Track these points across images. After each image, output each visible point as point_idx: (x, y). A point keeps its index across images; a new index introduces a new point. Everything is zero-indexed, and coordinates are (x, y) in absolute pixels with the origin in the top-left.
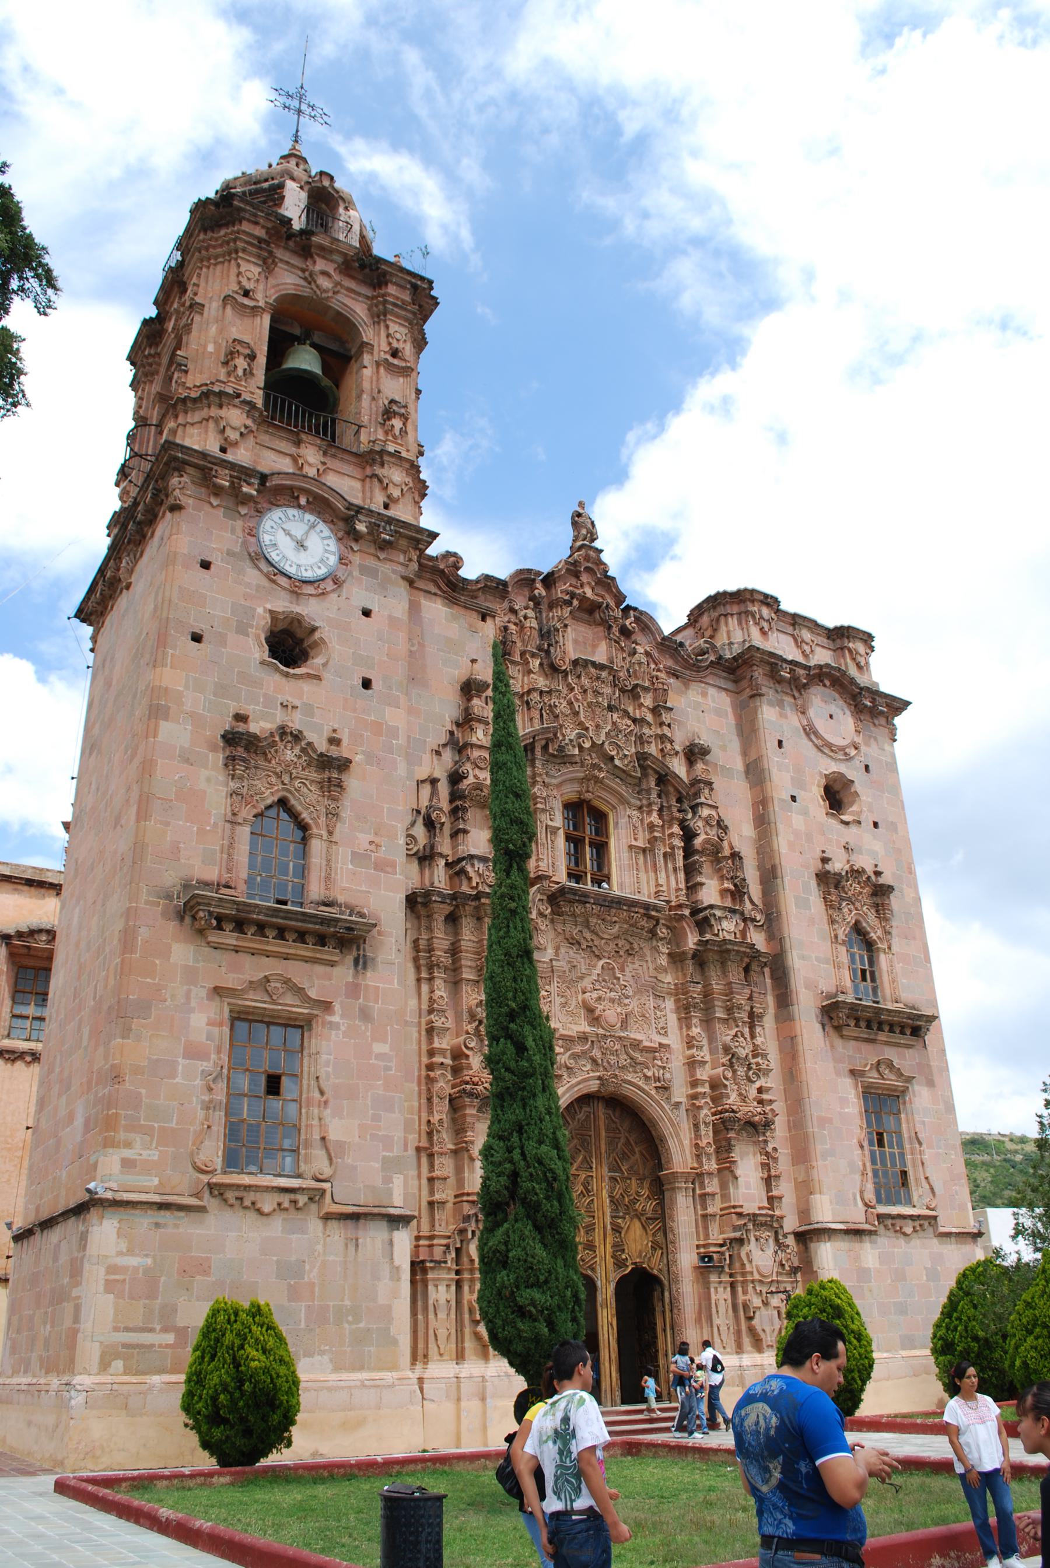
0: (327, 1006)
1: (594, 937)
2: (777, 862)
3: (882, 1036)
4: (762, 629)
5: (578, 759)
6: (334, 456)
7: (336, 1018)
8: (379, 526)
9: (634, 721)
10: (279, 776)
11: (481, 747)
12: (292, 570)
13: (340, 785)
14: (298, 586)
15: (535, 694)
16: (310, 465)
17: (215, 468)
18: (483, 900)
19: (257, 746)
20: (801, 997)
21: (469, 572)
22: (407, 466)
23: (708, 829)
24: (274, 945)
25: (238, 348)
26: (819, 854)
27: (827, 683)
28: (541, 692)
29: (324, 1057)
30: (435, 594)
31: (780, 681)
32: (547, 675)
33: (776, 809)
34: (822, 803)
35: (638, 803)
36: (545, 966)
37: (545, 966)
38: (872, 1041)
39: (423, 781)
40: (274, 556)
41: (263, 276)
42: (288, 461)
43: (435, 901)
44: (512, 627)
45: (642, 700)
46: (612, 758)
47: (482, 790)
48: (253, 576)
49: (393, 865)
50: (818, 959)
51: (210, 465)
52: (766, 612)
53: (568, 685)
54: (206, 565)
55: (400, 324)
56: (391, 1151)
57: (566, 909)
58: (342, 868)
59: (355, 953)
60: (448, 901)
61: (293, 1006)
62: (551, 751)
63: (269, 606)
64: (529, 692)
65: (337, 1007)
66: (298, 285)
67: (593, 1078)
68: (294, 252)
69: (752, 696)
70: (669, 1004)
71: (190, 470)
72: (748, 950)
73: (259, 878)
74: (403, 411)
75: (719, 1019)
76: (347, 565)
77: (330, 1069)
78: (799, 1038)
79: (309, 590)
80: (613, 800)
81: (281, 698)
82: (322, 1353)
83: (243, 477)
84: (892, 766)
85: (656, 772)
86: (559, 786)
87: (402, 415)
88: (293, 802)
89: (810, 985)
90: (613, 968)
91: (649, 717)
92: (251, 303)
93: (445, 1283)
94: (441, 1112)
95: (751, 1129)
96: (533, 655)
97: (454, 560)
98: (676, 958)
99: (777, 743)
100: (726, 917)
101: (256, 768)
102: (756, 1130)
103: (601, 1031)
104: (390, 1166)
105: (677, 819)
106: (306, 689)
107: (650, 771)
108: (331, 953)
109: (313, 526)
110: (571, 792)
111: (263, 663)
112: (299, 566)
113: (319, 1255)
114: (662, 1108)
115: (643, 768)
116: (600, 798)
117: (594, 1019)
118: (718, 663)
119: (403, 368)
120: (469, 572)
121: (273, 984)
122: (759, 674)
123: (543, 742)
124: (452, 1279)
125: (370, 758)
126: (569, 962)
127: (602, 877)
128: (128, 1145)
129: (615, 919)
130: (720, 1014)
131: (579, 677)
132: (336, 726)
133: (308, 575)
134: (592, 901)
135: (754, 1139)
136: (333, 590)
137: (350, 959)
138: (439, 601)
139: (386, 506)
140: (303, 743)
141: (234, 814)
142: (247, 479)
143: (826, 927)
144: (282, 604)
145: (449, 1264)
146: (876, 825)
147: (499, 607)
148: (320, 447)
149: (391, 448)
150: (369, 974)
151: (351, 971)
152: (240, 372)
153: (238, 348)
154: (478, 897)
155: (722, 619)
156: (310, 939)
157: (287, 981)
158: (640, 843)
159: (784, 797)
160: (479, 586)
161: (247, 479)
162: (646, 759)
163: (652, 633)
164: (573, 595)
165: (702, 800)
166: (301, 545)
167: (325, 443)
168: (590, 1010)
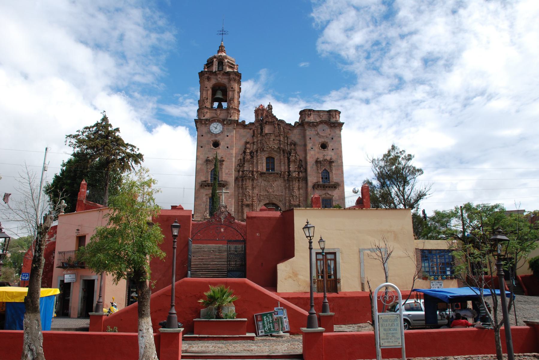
3: (327, 189)
12: (215, 133)
14: (216, 135)
21: (247, 123)
27: (323, 123)
38: (325, 190)
39: (239, 160)
40: (212, 131)
42: (215, 114)
44: (255, 130)
48: (209, 135)
52: (309, 113)
54: (202, 136)
57: (263, 175)
68: (215, 75)
70: (284, 187)
79: (218, 135)
80: (275, 155)
84: (340, 137)
86: (264, 155)
92: (207, 89)
94: (240, 207)
96: (259, 134)
97: (244, 122)
98: (285, 180)
109: (218, 125)
110: (267, 156)
115: (280, 149)
116: (273, 156)
117: (268, 192)
120: (247, 123)
122: (306, 126)
127: (273, 169)
128: (196, 214)
133: (218, 133)
139: (231, 117)
144: (214, 139)
146: (333, 150)
147: (253, 128)
154: (244, 177)
166: (216, 128)
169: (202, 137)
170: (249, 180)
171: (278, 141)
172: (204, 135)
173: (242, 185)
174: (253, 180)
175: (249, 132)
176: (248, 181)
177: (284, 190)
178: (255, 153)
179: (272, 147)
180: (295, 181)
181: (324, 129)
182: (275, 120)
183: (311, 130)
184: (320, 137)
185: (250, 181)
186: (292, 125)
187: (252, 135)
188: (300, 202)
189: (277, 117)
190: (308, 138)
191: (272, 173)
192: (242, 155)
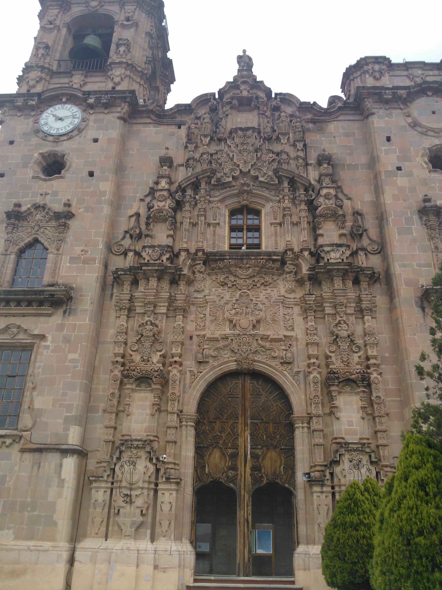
0: (42, 337)
1: (237, 279)
2: (383, 210)
4: (374, 78)
5: (234, 183)
6: (91, 76)
7: (48, 343)
8: (101, 97)
9: (278, 154)
10: (33, 228)
11: (161, 190)
12: (53, 132)
13: (65, 226)
15: (205, 156)
16: (76, 83)
17: (16, 99)
18: (143, 268)
19: (22, 217)
20: (402, 292)
22: (124, 65)
23: (327, 201)
24: (14, 309)
25: (40, 46)
26: (421, 197)
27: (430, 93)
28: (212, 155)
29: (37, 364)
30: (150, 123)
31: (387, 102)
32: (218, 145)
33: (383, 178)
34: (425, 166)
35: (278, 198)
36: (201, 300)
37: (201, 300)
39: (131, 216)
40: (45, 128)
41: (62, 12)
43: (121, 274)
44: (193, 126)
45: (282, 141)
46: (257, 177)
47: (163, 213)
48: (35, 140)
49: (94, 260)
50: (418, 265)
51: (14, 99)
52: (377, 67)
53: (228, 145)
54: (11, 143)
55: (132, 5)
56: (72, 413)
58: (63, 266)
59: (64, 308)
60: (128, 273)
61: (24, 339)
62: (212, 183)
63: (41, 151)
64: (202, 156)
65: (50, 338)
66: (82, 10)
67: (232, 361)
69: (367, 117)
70: (297, 309)
71: (7, 104)
72: (347, 267)
73: (20, 280)
74: (125, 42)
75: (328, 314)
76: (85, 121)
77: (40, 371)
78: (400, 320)
79: (65, 138)
81: (40, 192)
82: (9, 528)
83: (30, 98)
85: (287, 177)
87: (124, 44)
88: (40, 239)
89: (408, 283)
90: (248, 295)
91: (288, 148)
93: (103, 490)
95: (354, 385)
96: (206, 136)
98: (300, 282)
99: (385, 139)
100: (333, 250)
101: (22, 227)
102: (357, 384)
103: (237, 332)
104: (68, 421)
105: (304, 201)
106: (55, 184)
107: (284, 179)
108: (47, 310)
110: (233, 203)
111: (33, 178)
112: (58, 129)
113: (15, 472)
114: (285, 376)
115: (280, 178)
118: (345, 107)
119: (132, 24)
121: (12, 330)
122: (369, 104)
123: (206, 179)
124: (107, 488)
125: (87, 209)
126: (219, 296)
129: (248, 265)
130: (329, 310)
131: (233, 139)
132: (69, 198)
133: (63, 131)
134: (228, 257)
135: (357, 391)
136: (77, 135)
137: (61, 311)
138: (152, 125)
140: (46, 210)
141: (6, 251)
142: (32, 98)
143: (427, 243)
144: (47, 148)
145: (105, 478)
147: (188, 119)
148: (82, 74)
149: (117, 61)
150: (71, 318)
151: (60, 318)
152: (40, 55)
153: (40, 46)
155: (352, 82)
156: (34, 304)
157: (19, 327)
158: (278, 221)
159: (390, 169)
160: (173, 111)
161: (32, 98)
162: (278, 172)
163: (294, 104)
164: (232, 98)
165: (324, 185)
167: (85, 71)
168: (231, 321)
169: (11, 147)
170: (159, 279)
171: (271, 155)
172: (17, 140)
173: (131, 300)
174: (174, 282)
175: (172, 134)
176: (153, 283)
177: (299, 320)
178: (189, 192)
179: (252, 172)
180: (344, 283)
181: (435, 109)
182: (262, 95)
183: (390, 115)
184: (422, 133)
185: (165, 285)
186: (320, 108)
187: (185, 140)
188: (368, 367)
189: (267, 84)
190: (380, 139)
191: (248, 255)
192: (142, 200)
